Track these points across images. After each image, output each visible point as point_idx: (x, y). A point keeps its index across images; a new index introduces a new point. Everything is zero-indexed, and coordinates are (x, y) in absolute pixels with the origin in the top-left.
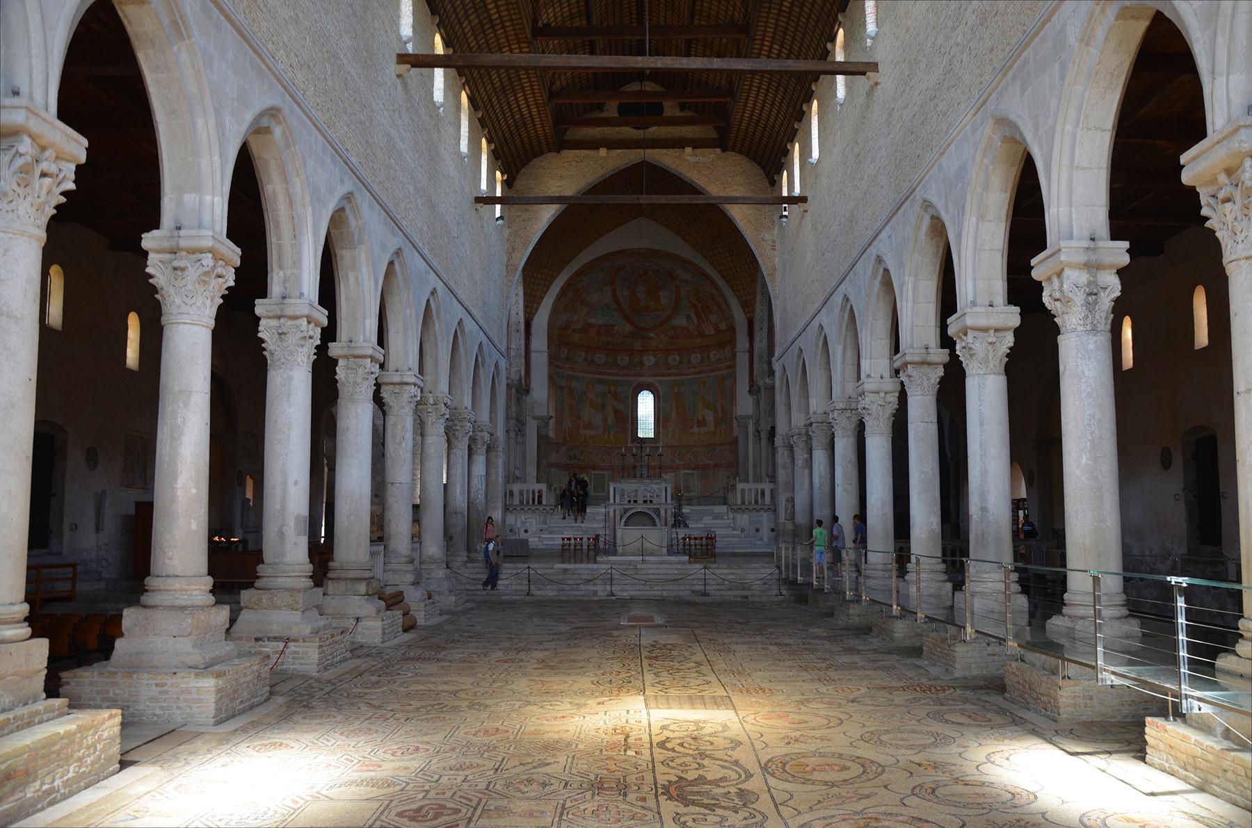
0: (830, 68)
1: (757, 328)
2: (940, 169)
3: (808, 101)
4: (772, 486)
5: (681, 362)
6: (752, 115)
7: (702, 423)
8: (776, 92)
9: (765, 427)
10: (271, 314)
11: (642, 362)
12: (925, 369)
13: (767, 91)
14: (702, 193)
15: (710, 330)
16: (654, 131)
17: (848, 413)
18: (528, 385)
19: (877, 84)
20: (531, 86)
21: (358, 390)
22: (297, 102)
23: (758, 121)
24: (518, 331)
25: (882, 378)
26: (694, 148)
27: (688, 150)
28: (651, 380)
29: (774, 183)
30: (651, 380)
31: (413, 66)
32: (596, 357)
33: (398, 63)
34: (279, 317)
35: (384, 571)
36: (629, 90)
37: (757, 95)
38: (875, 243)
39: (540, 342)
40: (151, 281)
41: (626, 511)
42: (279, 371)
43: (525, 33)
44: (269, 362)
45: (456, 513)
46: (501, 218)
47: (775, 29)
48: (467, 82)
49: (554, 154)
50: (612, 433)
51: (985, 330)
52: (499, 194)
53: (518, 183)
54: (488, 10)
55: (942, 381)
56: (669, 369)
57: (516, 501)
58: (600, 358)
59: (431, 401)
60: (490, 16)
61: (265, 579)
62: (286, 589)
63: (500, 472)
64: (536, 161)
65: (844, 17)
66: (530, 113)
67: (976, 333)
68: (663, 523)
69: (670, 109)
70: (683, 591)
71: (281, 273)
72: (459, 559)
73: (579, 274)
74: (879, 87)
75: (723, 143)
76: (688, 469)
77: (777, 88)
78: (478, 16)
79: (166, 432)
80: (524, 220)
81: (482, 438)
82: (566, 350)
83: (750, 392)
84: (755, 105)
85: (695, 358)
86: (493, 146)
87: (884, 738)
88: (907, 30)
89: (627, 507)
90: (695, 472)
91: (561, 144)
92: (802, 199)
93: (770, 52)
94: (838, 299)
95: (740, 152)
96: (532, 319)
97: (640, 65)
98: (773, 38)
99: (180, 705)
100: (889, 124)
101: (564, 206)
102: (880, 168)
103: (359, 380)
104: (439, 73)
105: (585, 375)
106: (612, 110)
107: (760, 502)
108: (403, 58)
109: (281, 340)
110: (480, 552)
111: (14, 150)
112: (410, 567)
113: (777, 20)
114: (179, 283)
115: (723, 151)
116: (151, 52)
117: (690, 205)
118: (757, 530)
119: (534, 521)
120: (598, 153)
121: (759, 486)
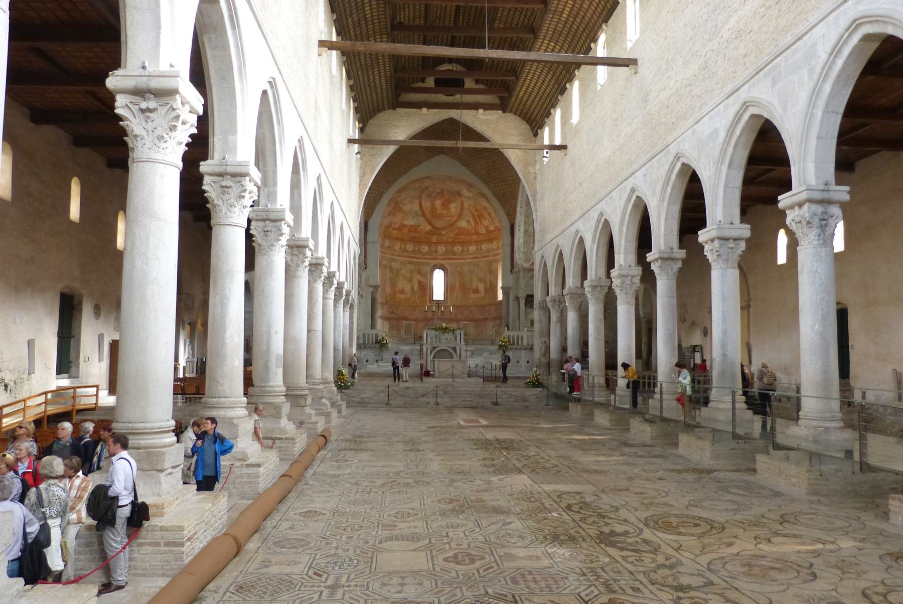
0: (595, 61)
1: (516, 230)
2: (694, 133)
3: (570, 79)
4: (529, 333)
5: (463, 251)
6: (527, 89)
7: (476, 291)
8: (547, 74)
9: (523, 295)
10: (259, 218)
12: (670, 263)
13: (541, 73)
14: (489, 141)
15: (482, 231)
16: (457, 98)
17: (599, 289)
18: (365, 264)
19: (636, 73)
20: (384, 64)
21: (300, 269)
22: (280, 73)
23: (531, 94)
25: (630, 266)
26: (485, 109)
27: (481, 111)
28: (443, 262)
29: (536, 134)
30: (443, 262)
31: (329, 49)
33: (319, 46)
34: (264, 220)
36: (442, 69)
37: (533, 76)
38: (631, 179)
40: (205, 195)
41: (434, 348)
42: (265, 257)
43: (387, 28)
44: (257, 250)
46: (358, 153)
47: (554, 32)
48: (347, 60)
49: (391, 111)
51: (727, 239)
52: (357, 138)
53: (369, 129)
54: (365, 11)
55: (681, 270)
57: (361, 342)
58: (410, 247)
60: (365, 15)
61: (255, 397)
62: (270, 404)
64: (380, 115)
65: (607, 26)
67: (722, 242)
68: (458, 356)
69: (469, 83)
71: (266, 190)
73: (400, 191)
74: (637, 75)
75: (503, 106)
76: (467, 321)
77: (548, 72)
78: (358, 15)
79: (217, 299)
80: (371, 155)
82: (388, 242)
83: (511, 271)
84: (535, 85)
85: (472, 248)
87: (704, 504)
88: (666, 38)
90: (472, 323)
91: (396, 104)
92: (563, 147)
93: (547, 47)
94: (595, 214)
95: (515, 114)
97: (482, 55)
98: (551, 38)
99: (236, 486)
100: (646, 101)
101: (398, 147)
102: (636, 129)
103: (300, 263)
104: (334, 52)
106: (430, 82)
107: (520, 343)
108: (322, 44)
109: (266, 235)
111: (169, 106)
113: (556, 26)
114: (226, 197)
115: (504, 111)
116: (213, 36)
117: (476, 148)
118: (518, 362)
119: (372, 354)
121: (520, 334)
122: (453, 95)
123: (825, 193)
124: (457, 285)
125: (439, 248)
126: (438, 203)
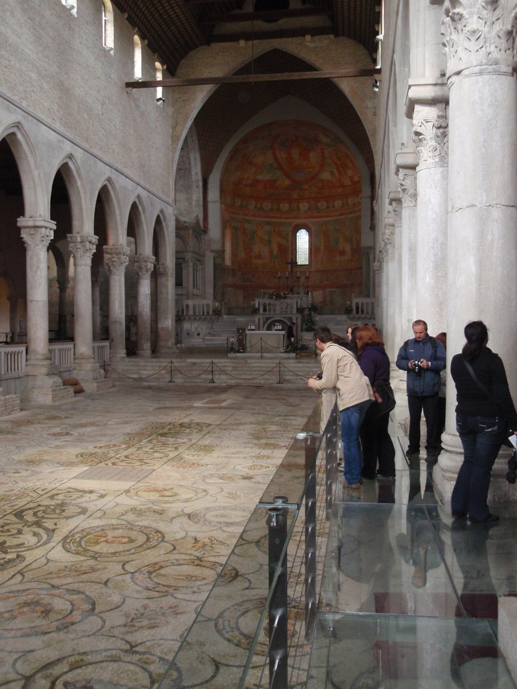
5: (328, 207)
7: (342, 253)
11: (298, 208)
15: (347, 182)
16: (284, 23)
24: (197, 187)
26: (313, 35)
27: (308, 37)
32: (264, 205)
35: (26, 365)
39: (214, 194)
41: (268, 319)
45: (116, 322)
50: (276, 261)
56: (319, 213)
58: (267, 205)
59: (79, 239)
63: (170, 292)
64: (192, 53)
66: (175, 13)
70: (273, 380)
72: (119, 356)
73: (245, 141)
80: (184, 101)
81: (146, 266)
85: (338, 204)
86: (146, 42)
89: (268, 316)
95: (349, 37)
96: (208, 177)
105: (255, 219)
110: (146, 350)
112: (46, 362)
115: (337, 35)
119: (204, 327)
120: (239, 44)
122: (275, 21)
123: (438, 88)
124: (322, 248)
125: (301, 205)
126: (295, 153)
